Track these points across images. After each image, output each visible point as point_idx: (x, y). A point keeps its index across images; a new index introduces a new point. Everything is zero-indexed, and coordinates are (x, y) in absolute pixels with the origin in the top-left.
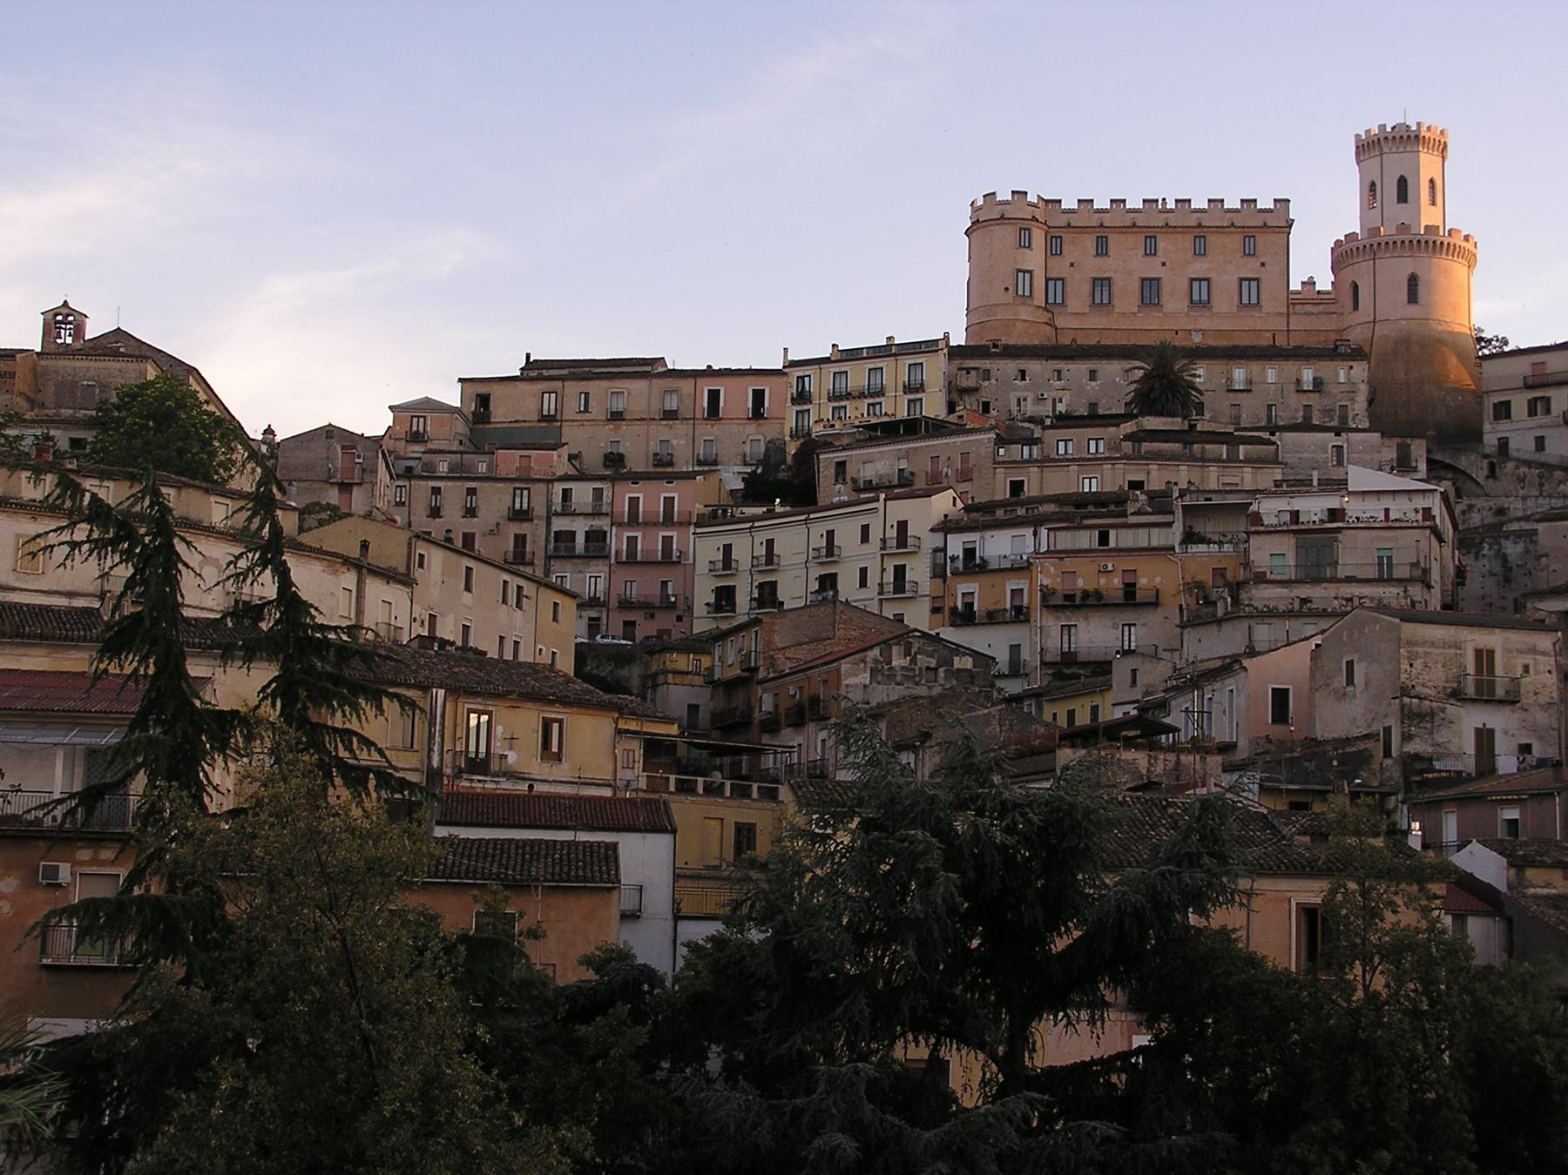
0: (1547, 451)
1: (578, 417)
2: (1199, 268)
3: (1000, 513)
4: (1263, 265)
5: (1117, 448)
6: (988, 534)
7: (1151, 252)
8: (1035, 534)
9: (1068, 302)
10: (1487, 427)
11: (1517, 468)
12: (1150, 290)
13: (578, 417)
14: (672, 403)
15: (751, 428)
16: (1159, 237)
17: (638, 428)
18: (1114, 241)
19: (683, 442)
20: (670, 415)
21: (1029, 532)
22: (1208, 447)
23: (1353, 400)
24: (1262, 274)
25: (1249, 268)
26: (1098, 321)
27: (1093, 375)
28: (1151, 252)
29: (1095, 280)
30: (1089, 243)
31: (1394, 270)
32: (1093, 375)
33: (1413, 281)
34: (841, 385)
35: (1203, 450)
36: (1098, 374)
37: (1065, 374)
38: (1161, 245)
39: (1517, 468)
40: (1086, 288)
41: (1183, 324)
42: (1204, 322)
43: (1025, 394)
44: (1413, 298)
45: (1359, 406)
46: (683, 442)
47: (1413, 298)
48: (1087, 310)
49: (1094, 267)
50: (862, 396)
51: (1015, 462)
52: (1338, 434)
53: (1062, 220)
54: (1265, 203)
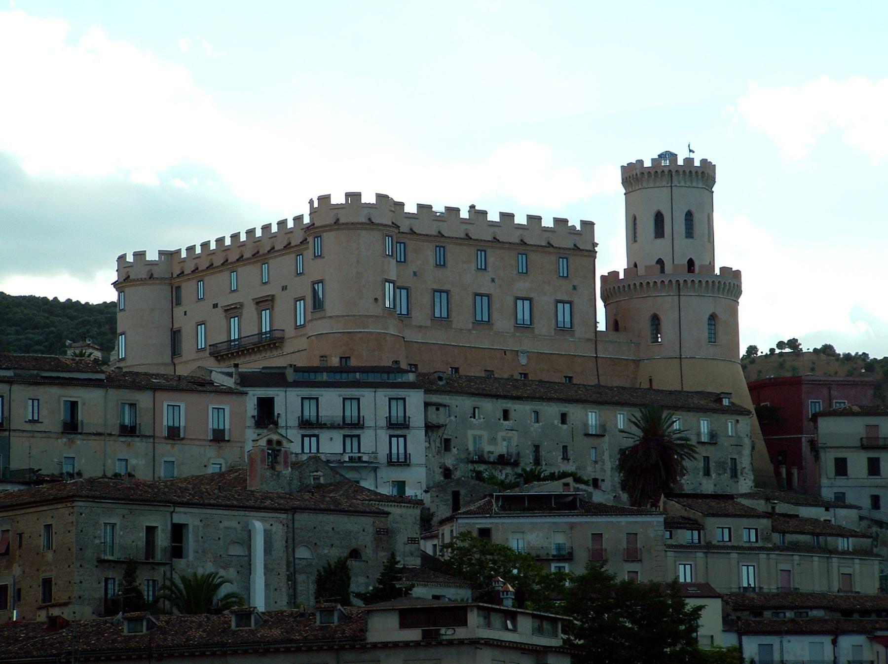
0: (882, 510)
1: (28, 427)
2: (522, 287)
3: (768, 614)
4: (575, 288)
5: (767, 539)
6: (786, 638)
8: (834, 642)
9: (414, 314)
10: (824, 481)
11: (869, 527)
13: (28, 427)
15: (211, 452)
16: (489, 251)
17: (94, 444)
19: (142, 462)
20: (129, 431)
21: (827, 640)
22: (829, 539)
23: (740, 453)
24: (576, 300)
26: (438, 337)
29: (435, 291)
31: (698, 307)
33: (713, 317)
34: (310, 412)
35: (826, 541)
36: (541, 418)
37: (512, 414)
38: (491, 260)
39: (869, 527)
40: (427, 299)
41: (511, 345)
42: (527, 345)
43: (479, 432)
44: (713, 339)
46: (142, 462)
47: (713, 339)
48: (429, 323)
50: (333, 427)
51: (681, 546)
52: (827, 509)
54: (575, 222)
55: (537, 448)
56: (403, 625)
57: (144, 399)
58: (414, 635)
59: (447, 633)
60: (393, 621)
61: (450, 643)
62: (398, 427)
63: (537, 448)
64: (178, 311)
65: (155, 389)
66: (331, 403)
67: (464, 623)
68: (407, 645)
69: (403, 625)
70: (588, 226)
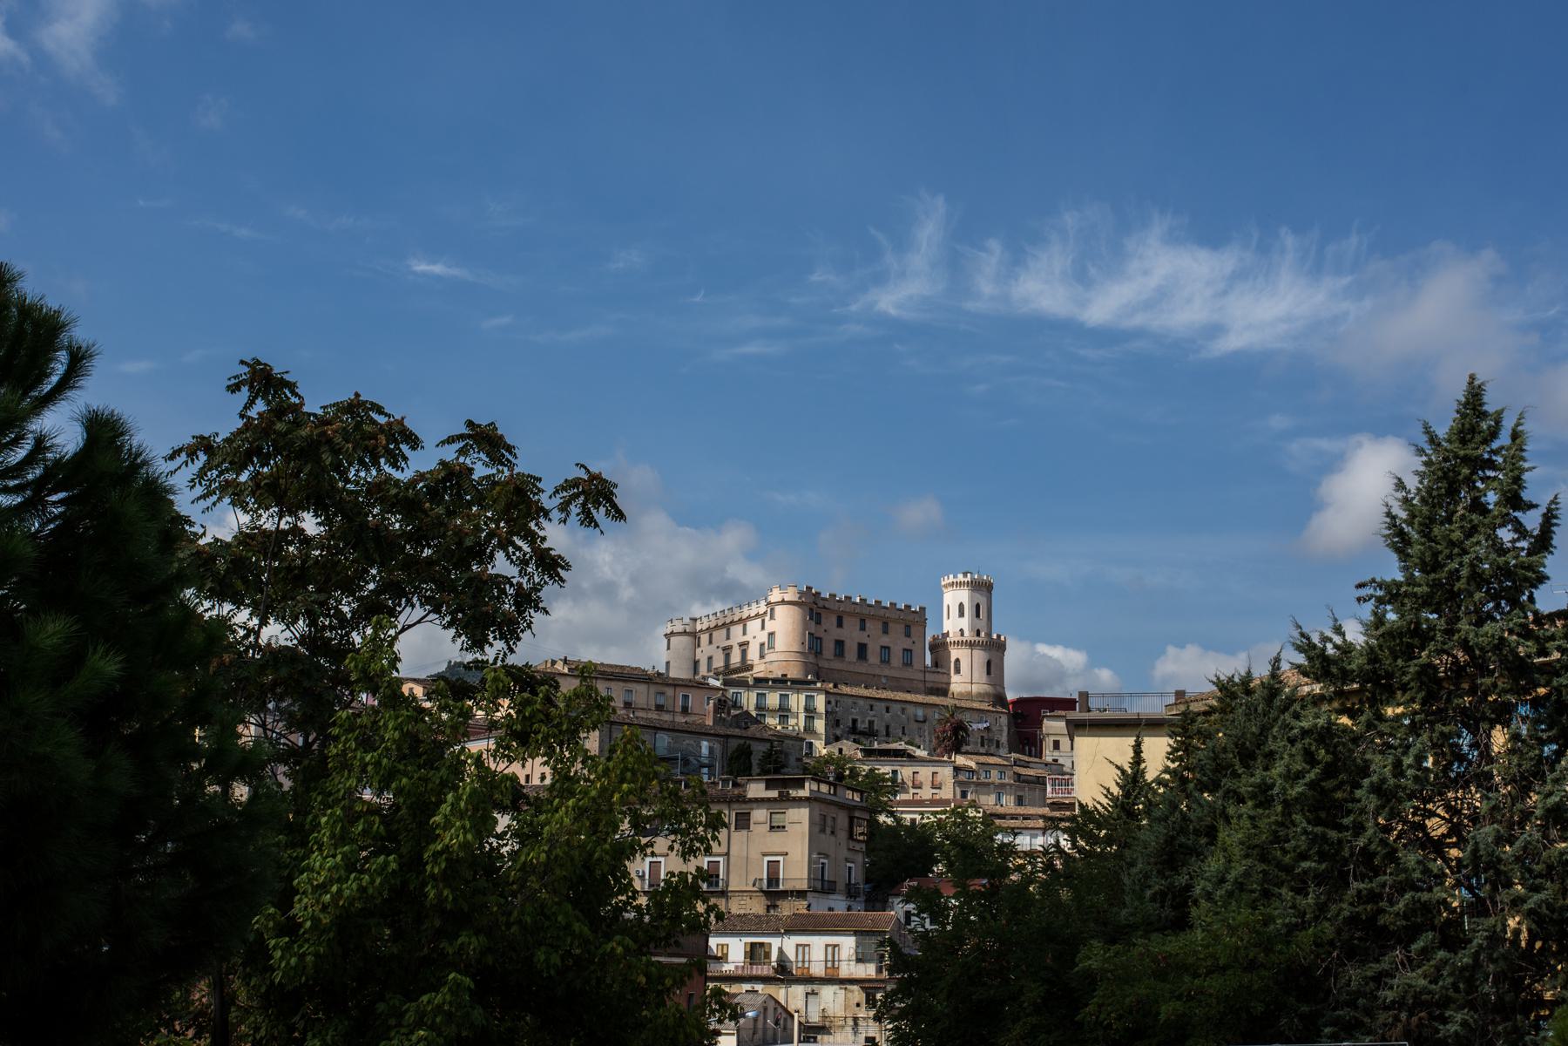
2: (885, 640)
7: (863, 628)
12: (862, 648)
14: (661, 701)
18: (845, 621)
25: (907, 643)
27: (888, 710)
28: (863, 628)
30: (834, 620)
32: (888, 710)
38: (868, 625)
40: (832, 645)
41: (878, 672)
42: (887, 672)
45: (1004, 739)
49: (837, 633)
53: (821, 604)
55: (887, 727)
56: (767, 788)
57: (670, 691)
58: (774, 794)
59: (793, 793)
60: (762, 786)
61: (794, 799)
62: (810, 712)
63: (887, 727)
64: (698, 651)
65: (675, 686)
66: (773, 699)
67: (803, 787)
68: (769, 800)
69: (767, 788)
70: (923, 609)
